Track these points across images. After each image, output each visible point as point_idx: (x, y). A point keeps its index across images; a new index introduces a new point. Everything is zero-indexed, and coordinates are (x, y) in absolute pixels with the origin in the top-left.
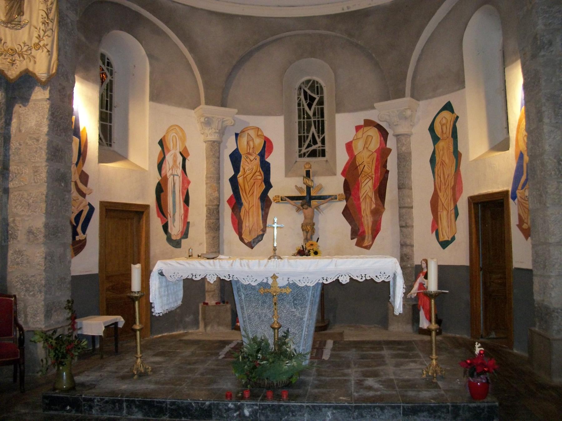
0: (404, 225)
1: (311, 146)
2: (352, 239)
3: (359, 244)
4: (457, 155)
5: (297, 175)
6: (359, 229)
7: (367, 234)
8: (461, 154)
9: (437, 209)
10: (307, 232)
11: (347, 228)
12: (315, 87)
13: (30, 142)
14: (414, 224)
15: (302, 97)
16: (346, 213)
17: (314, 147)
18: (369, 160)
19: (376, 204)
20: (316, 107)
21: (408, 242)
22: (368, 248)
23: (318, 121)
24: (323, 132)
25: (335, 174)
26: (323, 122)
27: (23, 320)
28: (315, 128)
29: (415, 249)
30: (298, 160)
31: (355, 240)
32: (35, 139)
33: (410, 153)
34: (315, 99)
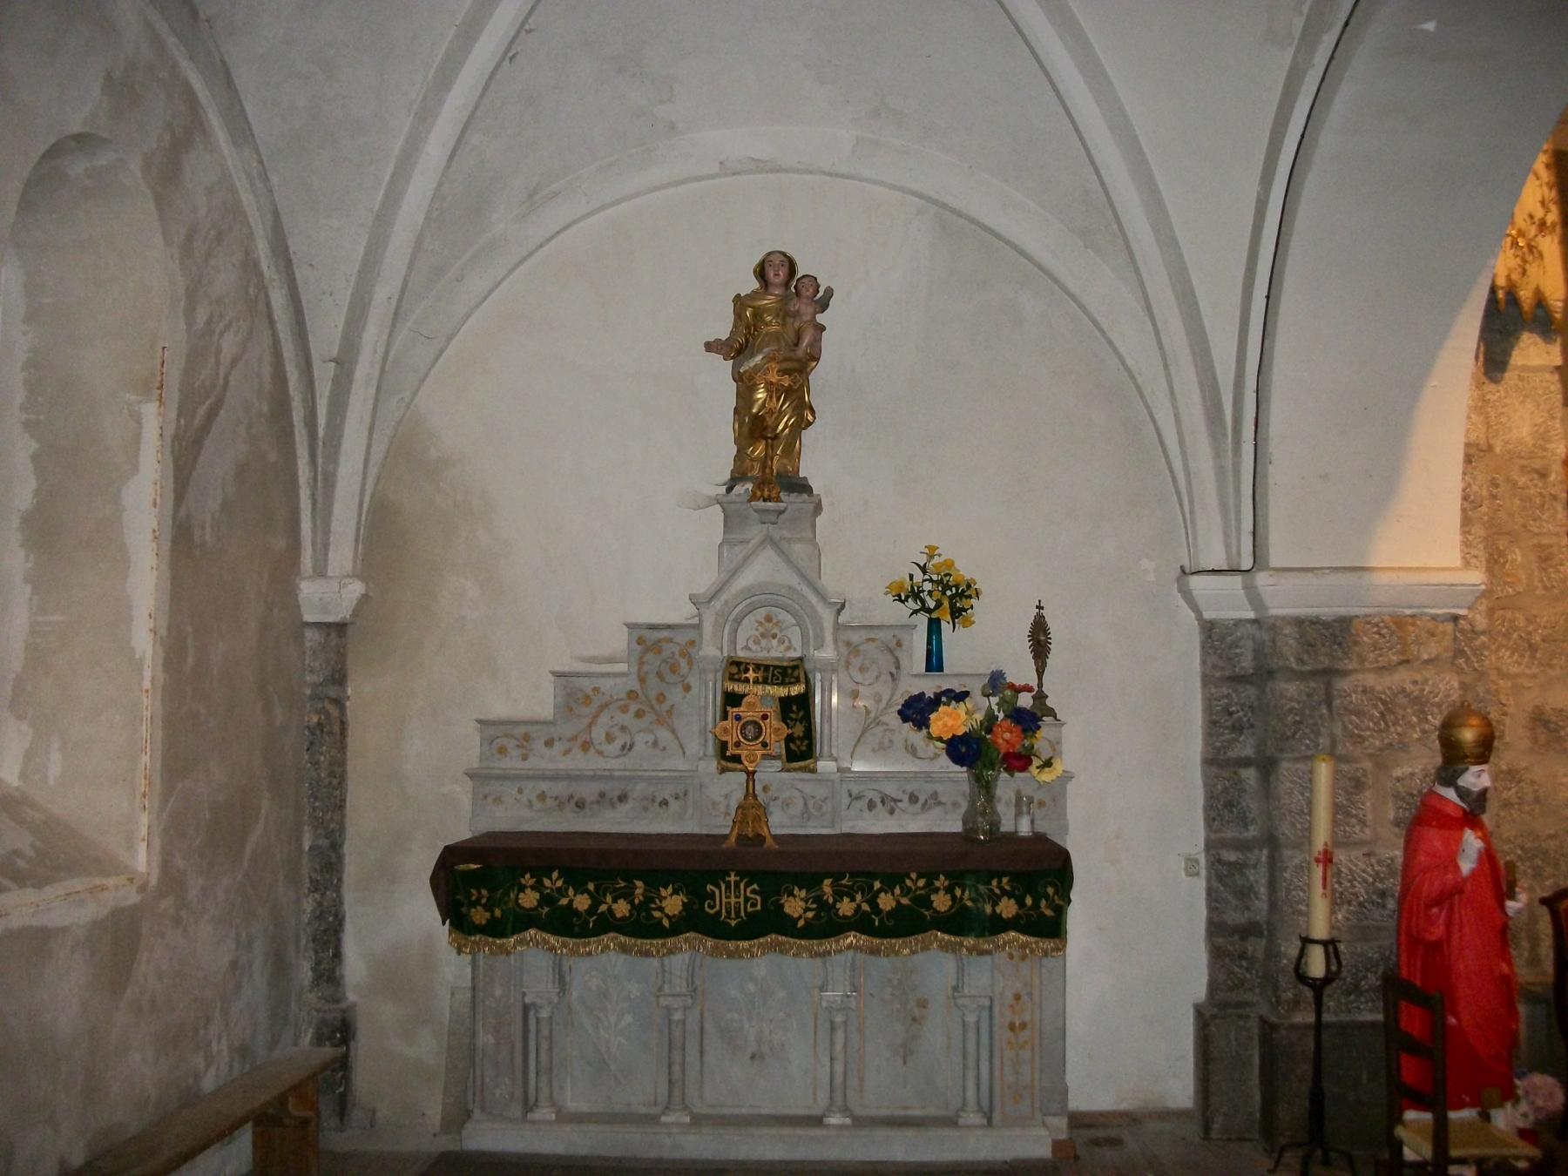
13: (1522, 480)
27: (1526, 954)
32: (1537, 471)
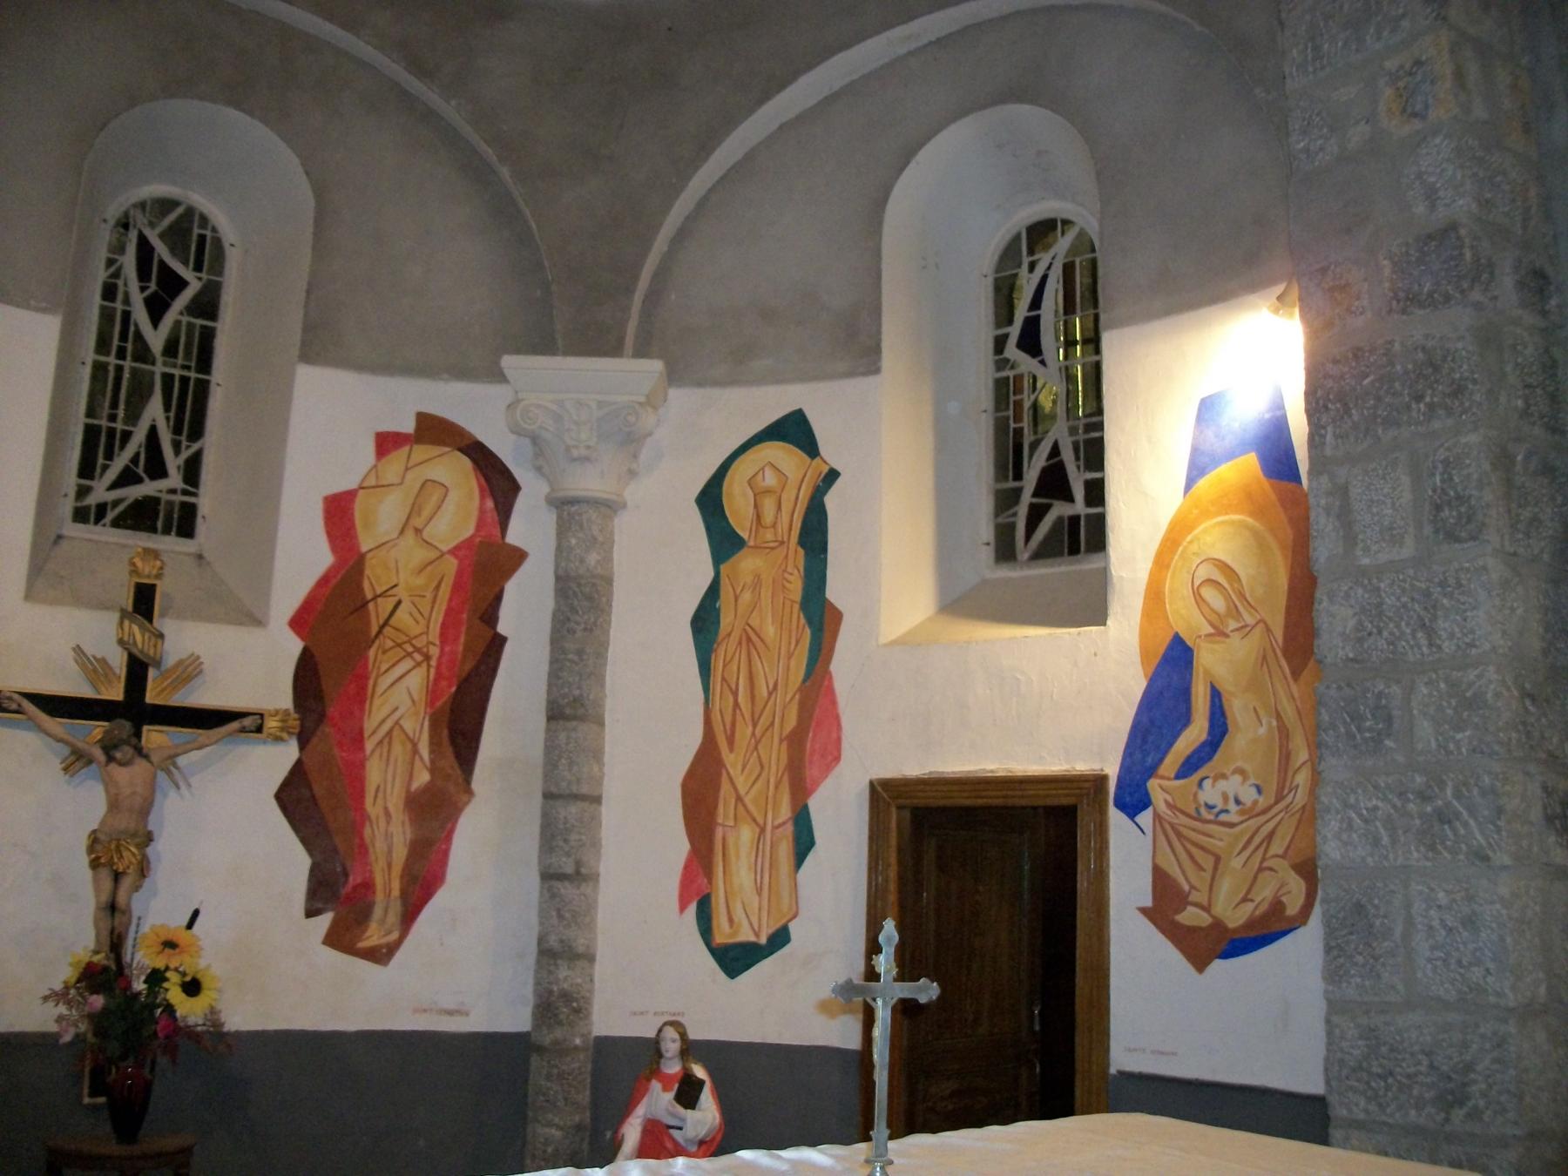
0: (569, 869)
1: (139, 481)
2: (311, 913)
3: (339, 939)
4: (821, 619)
5: (80, 600)
6: (346, 875)
7: (379, 897)
8: (838, 616)
9: (712, 813)
10: (117, 877)
11: (293, 862)
12: (194, 238)
14: (602, 870)
15: (129, 261)
16: (295, 797)
17: (148, 488)
18: (420, 581)
19: (433, 770)
20: (185, 319)
21: (580, 945)
22: (380, 955)
23: (185, 381)
24: (197, 432)
25: (255, 620)
26: (203, 389)
28: (167, 408)
29: (598, 969)
30: (65, 532)
31: (325, 921)
33: (609, 581)
34: (183, 284)
